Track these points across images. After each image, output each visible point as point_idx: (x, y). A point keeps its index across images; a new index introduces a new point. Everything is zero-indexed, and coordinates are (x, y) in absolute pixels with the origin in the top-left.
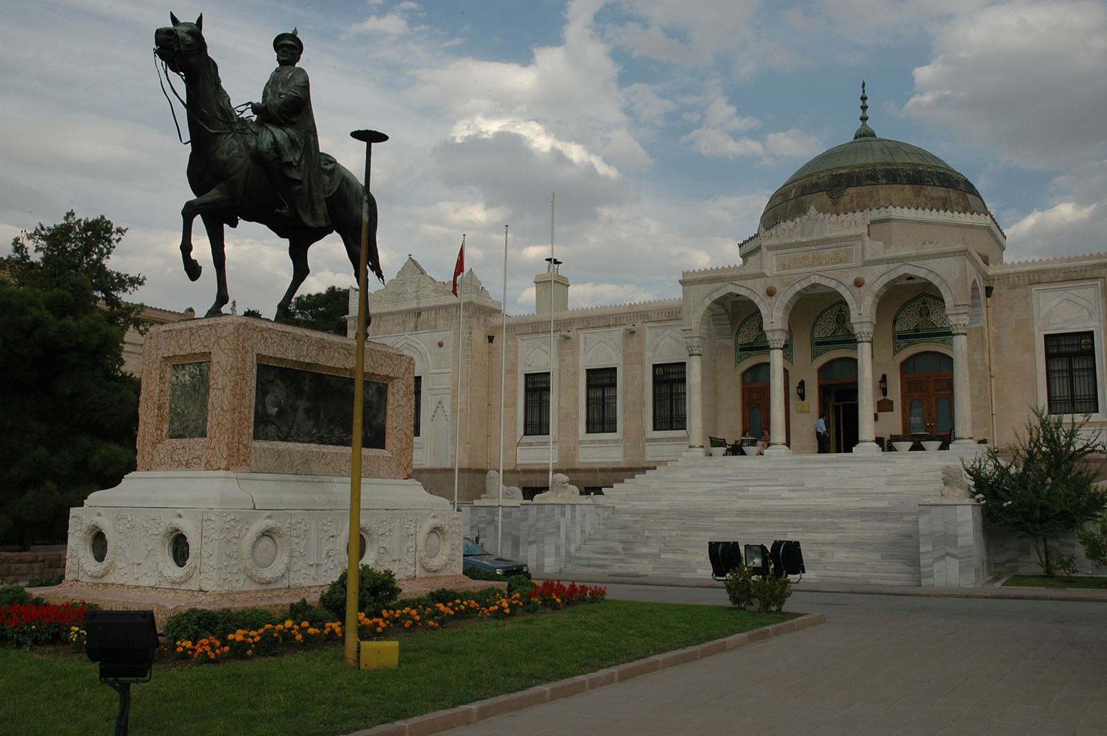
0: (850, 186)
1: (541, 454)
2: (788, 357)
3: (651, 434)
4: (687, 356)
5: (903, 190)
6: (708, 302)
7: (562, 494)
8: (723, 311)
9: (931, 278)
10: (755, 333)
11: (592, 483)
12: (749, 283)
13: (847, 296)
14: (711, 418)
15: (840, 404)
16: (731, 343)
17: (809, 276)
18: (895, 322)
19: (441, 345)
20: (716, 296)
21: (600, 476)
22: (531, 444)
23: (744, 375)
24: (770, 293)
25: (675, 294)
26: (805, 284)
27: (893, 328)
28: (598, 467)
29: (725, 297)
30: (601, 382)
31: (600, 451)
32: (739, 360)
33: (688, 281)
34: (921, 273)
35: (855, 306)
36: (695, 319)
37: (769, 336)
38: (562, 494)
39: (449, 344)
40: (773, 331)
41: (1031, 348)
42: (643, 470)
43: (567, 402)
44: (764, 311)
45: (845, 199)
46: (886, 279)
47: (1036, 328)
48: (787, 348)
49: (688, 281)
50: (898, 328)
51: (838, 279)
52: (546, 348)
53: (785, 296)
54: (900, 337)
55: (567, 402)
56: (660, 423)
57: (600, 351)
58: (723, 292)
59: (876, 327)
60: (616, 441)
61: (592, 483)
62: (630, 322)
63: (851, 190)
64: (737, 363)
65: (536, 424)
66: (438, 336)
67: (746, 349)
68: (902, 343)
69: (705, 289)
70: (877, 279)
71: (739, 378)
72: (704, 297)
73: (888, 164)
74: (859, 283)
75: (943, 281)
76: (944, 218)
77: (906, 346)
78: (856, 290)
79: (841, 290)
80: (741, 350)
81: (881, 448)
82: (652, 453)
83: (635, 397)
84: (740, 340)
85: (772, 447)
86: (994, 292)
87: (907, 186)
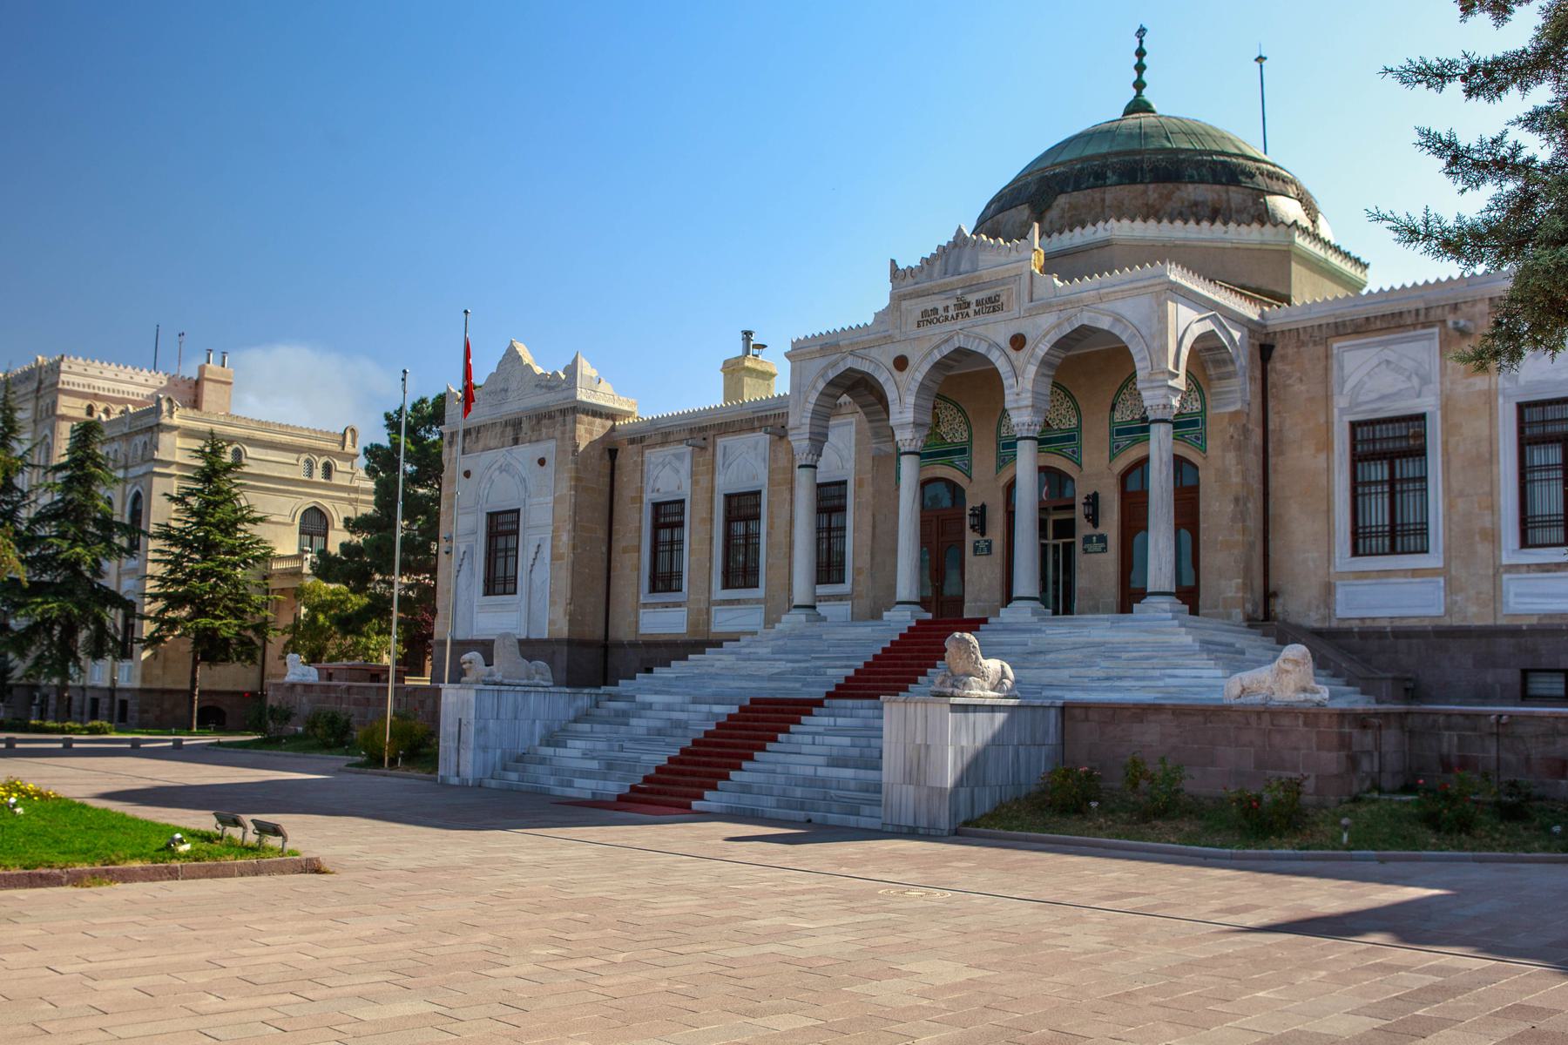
0: (1062, 192)
3: (719, 594)
5: (1145, 192)
6: (821, 385)
12: (874, 353)
15: (1060, 542)
17: (951, 337)
18: (1113, 408)
19: (542, 462)
20: (831, 375)
22: (738, 602)
24: (901, 363)
26: (946, 350)
27: (1111, 418)
35: (1012, 381)
39: (551, 461)
40: (902, 426)
41: (1327, 446)
45: (1053, 214)
47: (1336, 411)
50: (1118, 416)
51: (987, 336)
53: (919, 371)
54: (1119, 432)
58: (842, 368)
60: (758, 601)
63: (1062, 200)
66: (540, 450)
68: (1123, 440)
69: (820, 363)
70: (1044, 331)
73: (1132, 152)
74: (1018, 342)
76: (1181, 235)
77: (1127, 446)
81: (1187, 607)
82: (723, 621)
85: (1015, 604)
86: (1275, 354)
87: (1151, 186)
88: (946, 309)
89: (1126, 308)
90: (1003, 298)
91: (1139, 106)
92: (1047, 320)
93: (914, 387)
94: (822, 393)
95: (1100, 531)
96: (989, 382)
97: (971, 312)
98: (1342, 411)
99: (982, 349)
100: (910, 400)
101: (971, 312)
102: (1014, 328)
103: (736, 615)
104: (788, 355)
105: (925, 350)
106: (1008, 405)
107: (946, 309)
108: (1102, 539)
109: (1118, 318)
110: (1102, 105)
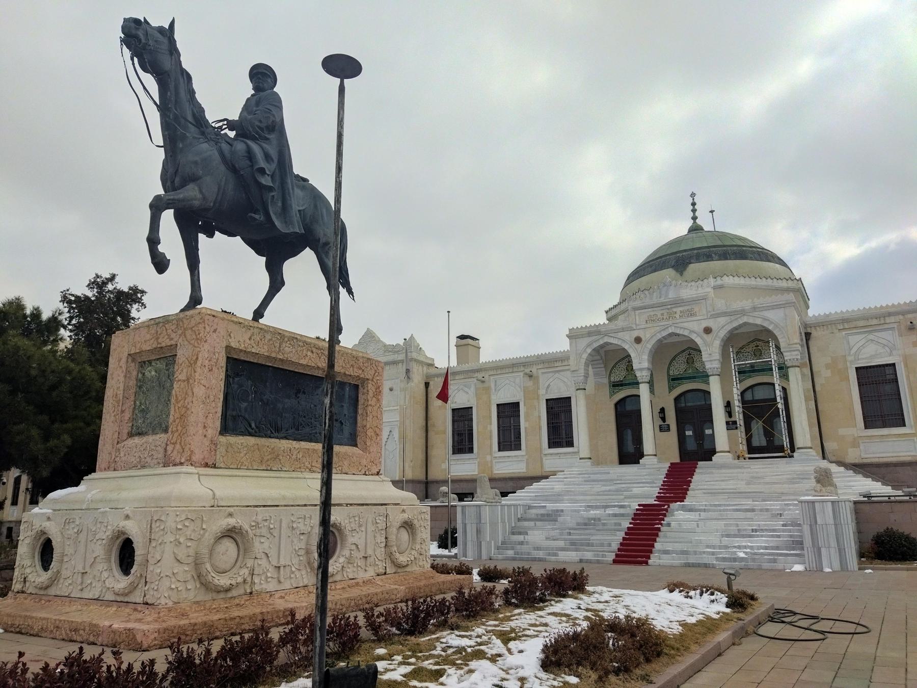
1: (463, 467)
2: (652, 391)
4: (574, 389)
7: (486, 493)
8: (599, 357)
9: (765, 324)
10: (624, 373)
11: (507, 486)
12: (620, 335)
13: (698, 341)
14: (593, 436)
16: (606, 381)
20: (595, 345)
21: (511, 484)
23: (616, 405)
25: (563, 345)
26: (664, 334)
28: (508, 476)
29: (602, 346)
30: (509, 413)
31: (511, 464)
32: (612, 394)
33: (574, 335)
34: (758, 321)
36: (578, 364)
37: (638, 374)
38: (486, 493)
40: (641, 370)
42: (547, 477)
43: (486, 428)
44: (633, 355)
46: (729, 328)
48: (651, 383)
49: (574, 335)
52: (466, 389)
53: (648, 345)
55: (486, 428)
56: (553, 444)
57: (508, 391)
58: (601, 342)
59: (722, 364)
61: (507, 486)
62: (526, 367)
64: (611, 396)
65: (463, 443)
67: (616, 386)
70: (722, 327)
71: (613, 407)
72: (586, 347)
75: (776, 326)
78: (705, 336)
79: (693, 337)
80: (614, 386)
83: (534, 423)
84: (612, 379)
88: (662, 314)
89: (772, 315)
90: (696, 309)
91: (695, 229)
92: (722, 320)
93: (647, 351)
94: (590, 354)
95: (733, 419)
96: (691, 351)
97: (677, 316)
98: (851, 362)
99: (686, 333)
100: (645, 357)
101: (677, 316)
102: (705, 324)
103: (555, 458)
104: (567, 336)
105: (652, 335)
106: (704, 360)
107: (662, 314)
108: (735, 423)
109: (765, 319)
110: (680, 228)
